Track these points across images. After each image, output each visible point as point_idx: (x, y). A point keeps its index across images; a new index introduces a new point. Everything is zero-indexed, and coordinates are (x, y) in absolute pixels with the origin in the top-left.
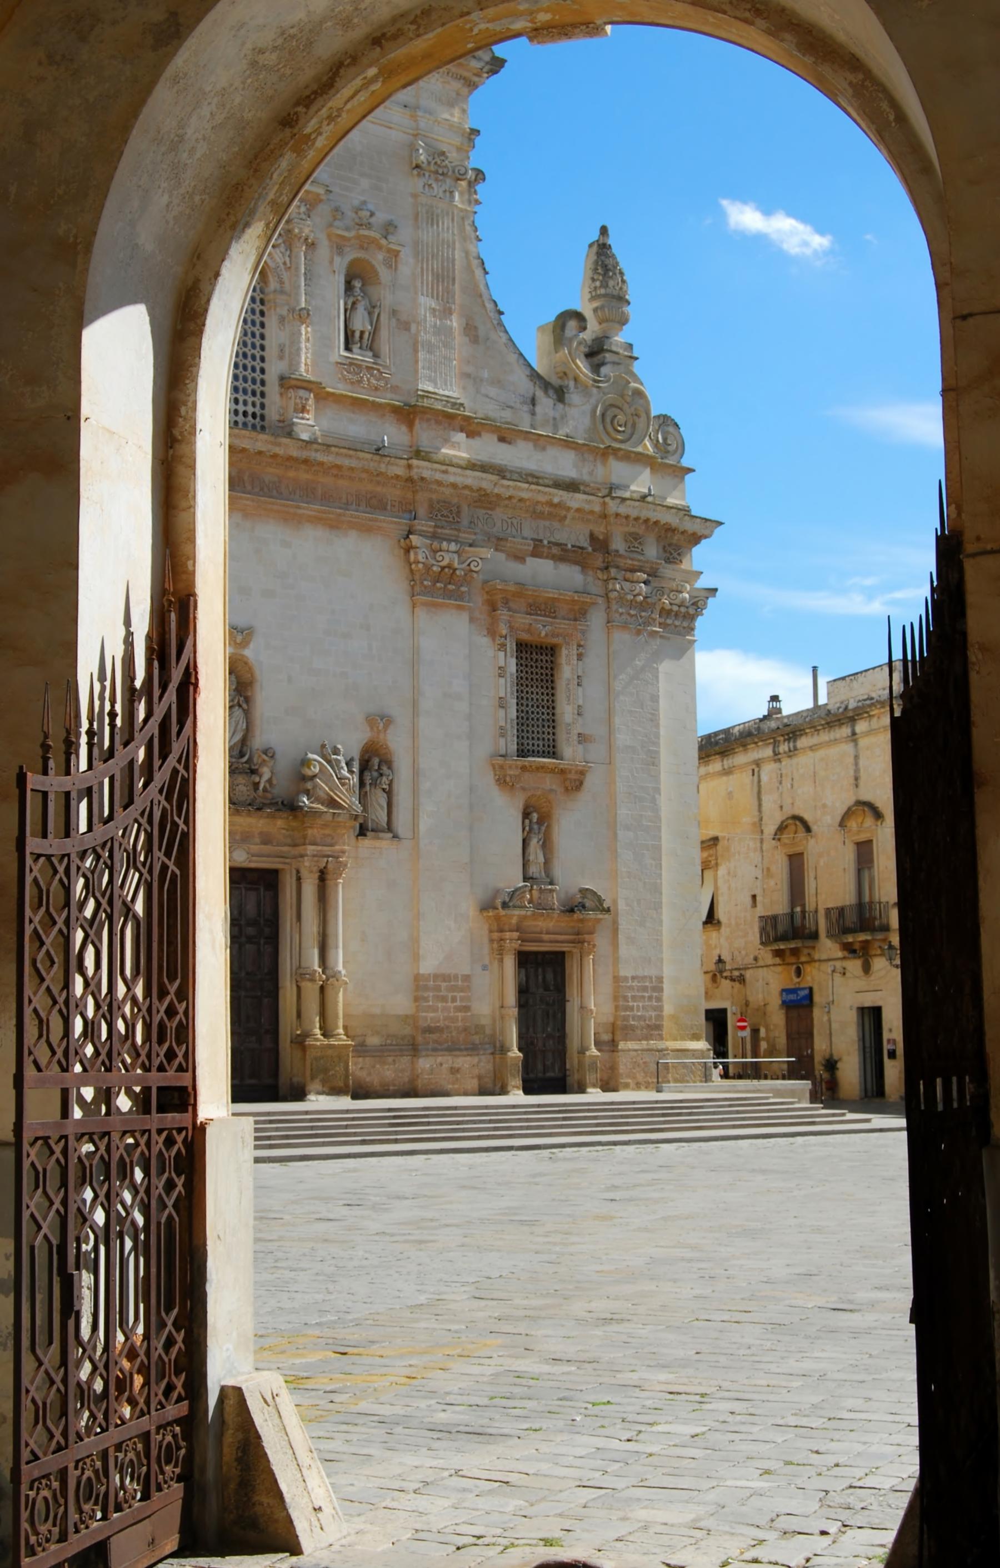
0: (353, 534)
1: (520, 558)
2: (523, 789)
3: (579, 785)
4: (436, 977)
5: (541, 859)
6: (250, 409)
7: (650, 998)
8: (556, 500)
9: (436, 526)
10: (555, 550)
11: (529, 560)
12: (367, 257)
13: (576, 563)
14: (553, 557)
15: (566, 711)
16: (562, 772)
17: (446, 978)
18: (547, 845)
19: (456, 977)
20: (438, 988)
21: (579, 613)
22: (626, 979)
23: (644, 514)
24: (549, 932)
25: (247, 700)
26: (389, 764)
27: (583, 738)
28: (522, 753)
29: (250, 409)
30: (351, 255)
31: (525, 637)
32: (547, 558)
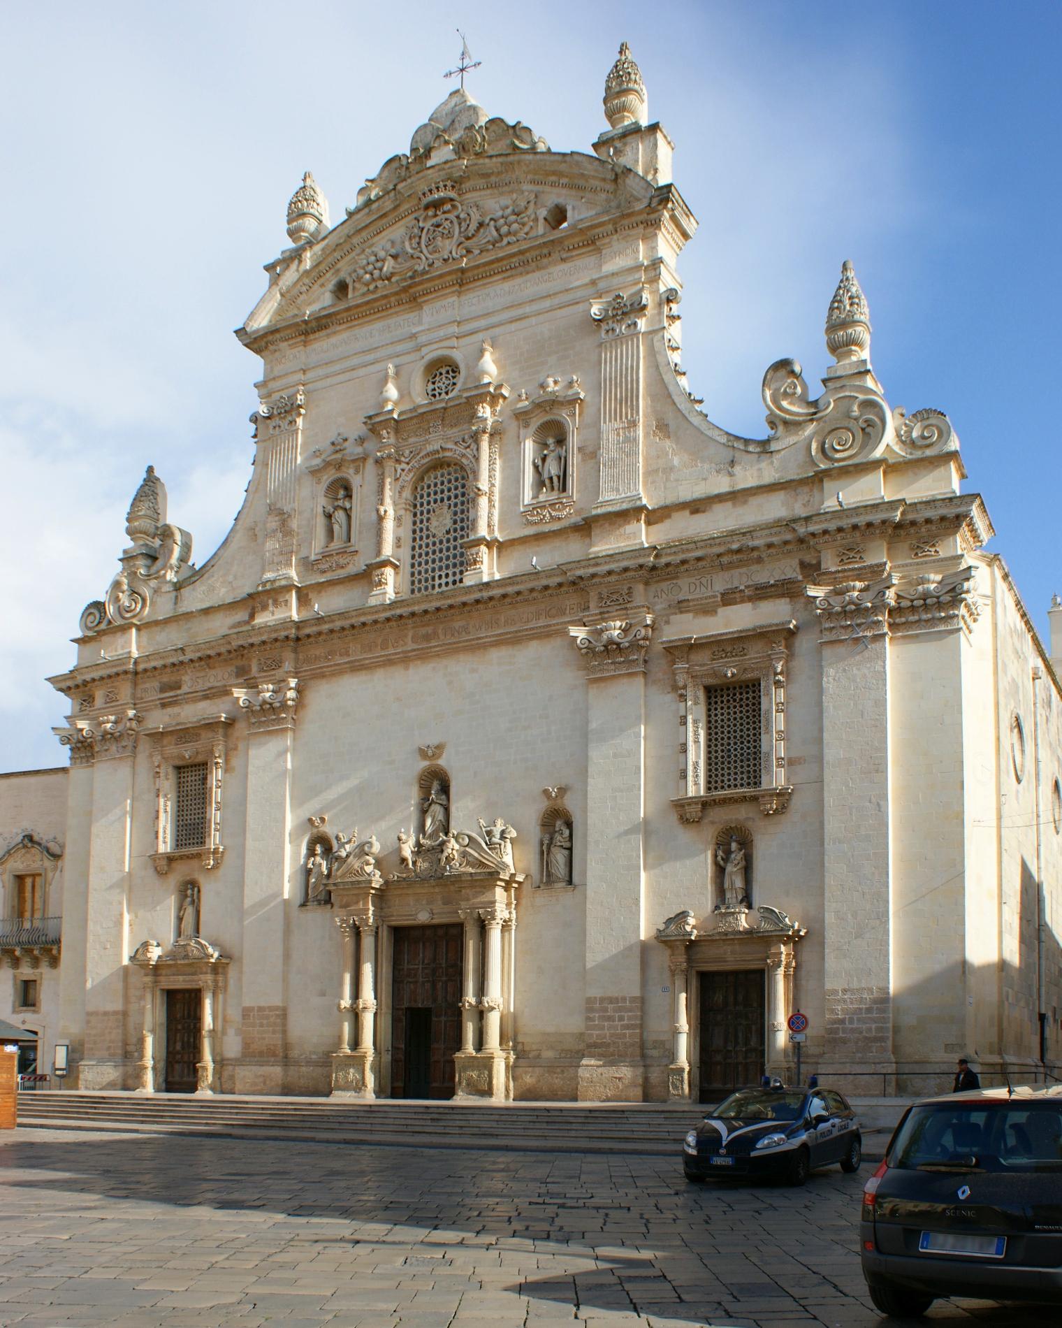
0: (534, 643)
2: (713, 823)
3: (782, 810)
4: (602, 1000)
5: (739, 883)
12: (552, 417)
13: (782, 596)
14: (750, 599)
16: (755, 799)
17: (611, 1000)
18: (747, 871)
19: (624, 999)
20: (606, 1010)
22: (835, 992)
23: (846, 523)
26: (569, 825)
30: (536, 422)
31: (711, 681)
32: (742, 602)
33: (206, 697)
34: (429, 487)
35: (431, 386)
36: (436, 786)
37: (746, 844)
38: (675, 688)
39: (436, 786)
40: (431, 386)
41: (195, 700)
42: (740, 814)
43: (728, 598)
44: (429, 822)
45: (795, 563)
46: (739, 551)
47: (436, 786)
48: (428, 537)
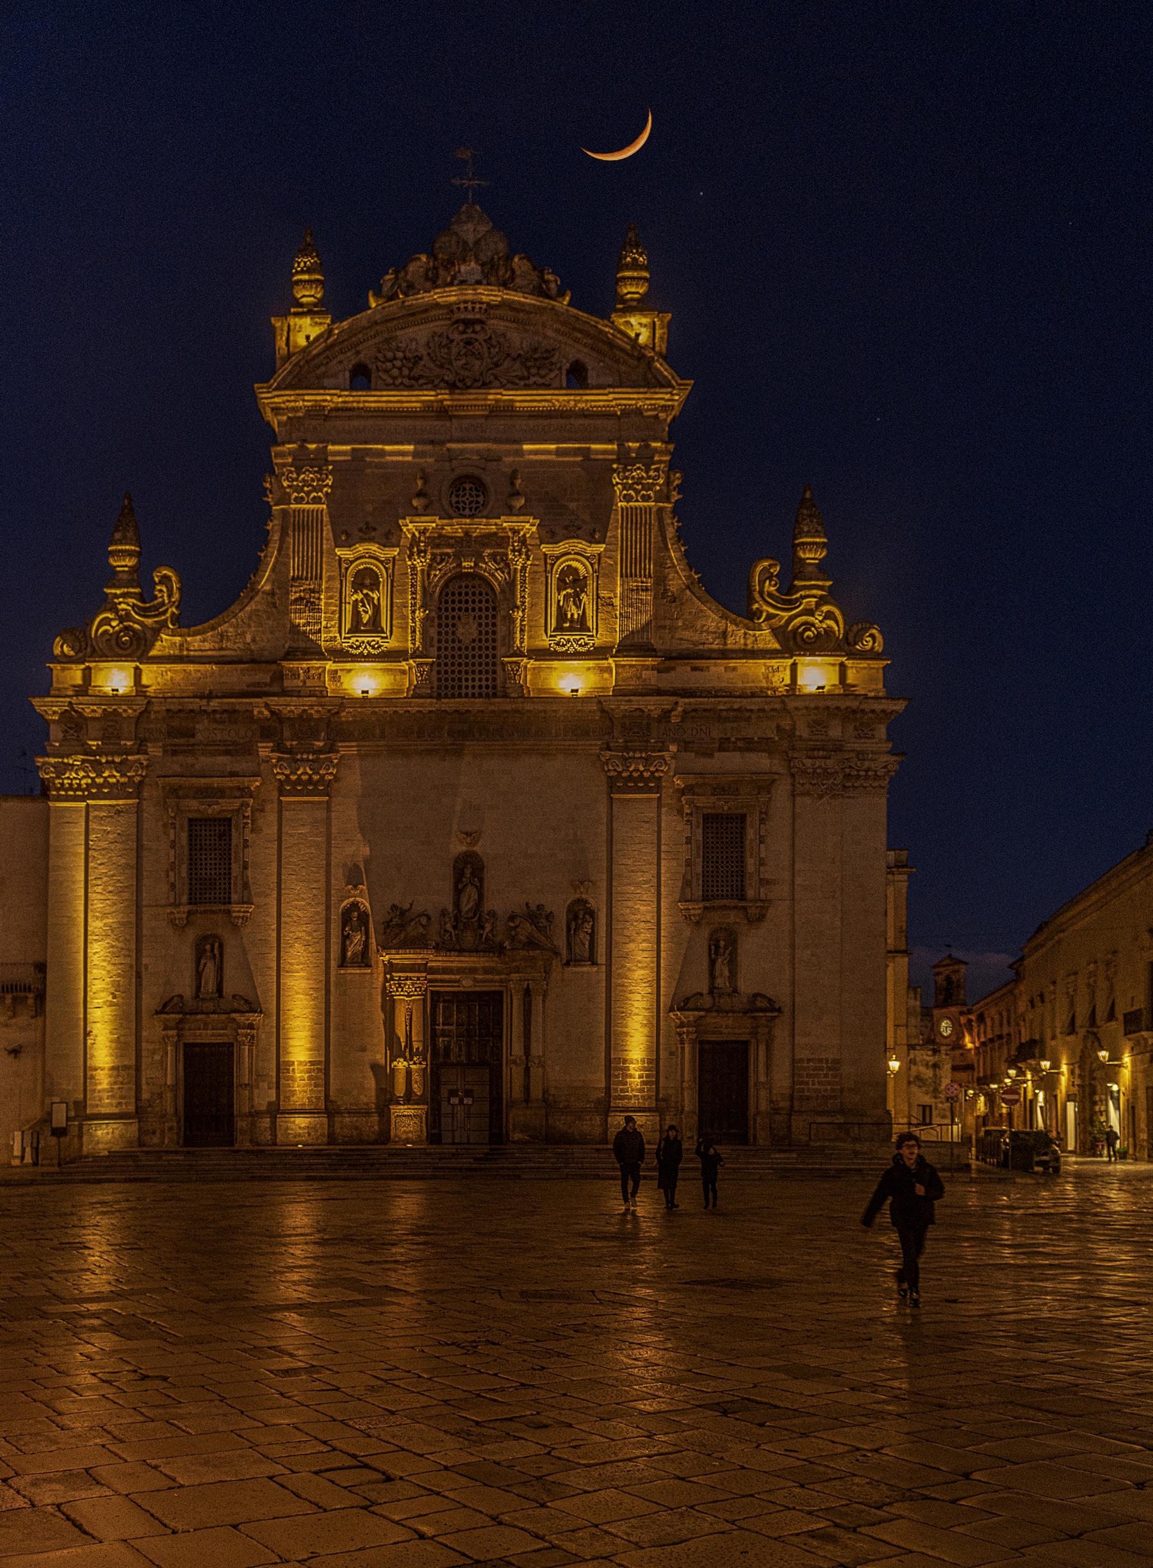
1: (711, 755)
3: (761, 918)
6: (484, 683)
7: (826, 1076)
8: (736, 706)
9: (626, 742)
10: (739, 744)
11: (716, 754)
14: (740, 750)
15: (751, 864)
18: (732, 963)
21: (764, 785)
24: (728, 1028)
25: (481, 880)
26: (592, 914)
27: (764, 882)
28: (705, 898)
29: (484, 683)
32: (734, 750)
33: (227, 753)
34: (453, 594)
35: (454, 499)
36: (468, 871)
37: (733, 942)
38: (680, 812)
39: (468, 871)
40: (454, 499)
41: (213, 754)
42: (732, 917)
43: (724, 745)
44: (464, 899)
45: (774, 726)
46: (739, 710)
47: (468, 872)
48: (453, 641)
